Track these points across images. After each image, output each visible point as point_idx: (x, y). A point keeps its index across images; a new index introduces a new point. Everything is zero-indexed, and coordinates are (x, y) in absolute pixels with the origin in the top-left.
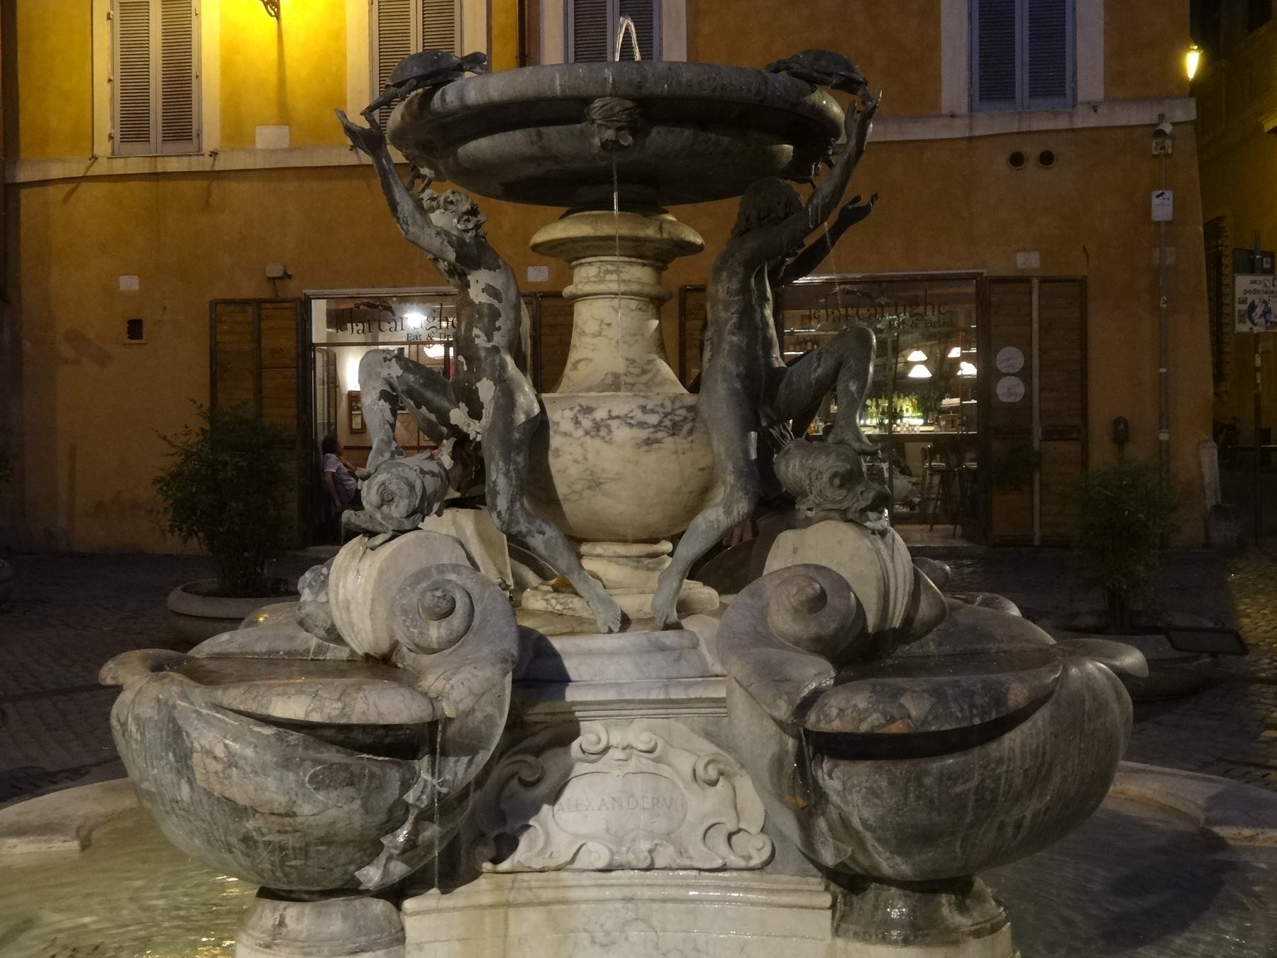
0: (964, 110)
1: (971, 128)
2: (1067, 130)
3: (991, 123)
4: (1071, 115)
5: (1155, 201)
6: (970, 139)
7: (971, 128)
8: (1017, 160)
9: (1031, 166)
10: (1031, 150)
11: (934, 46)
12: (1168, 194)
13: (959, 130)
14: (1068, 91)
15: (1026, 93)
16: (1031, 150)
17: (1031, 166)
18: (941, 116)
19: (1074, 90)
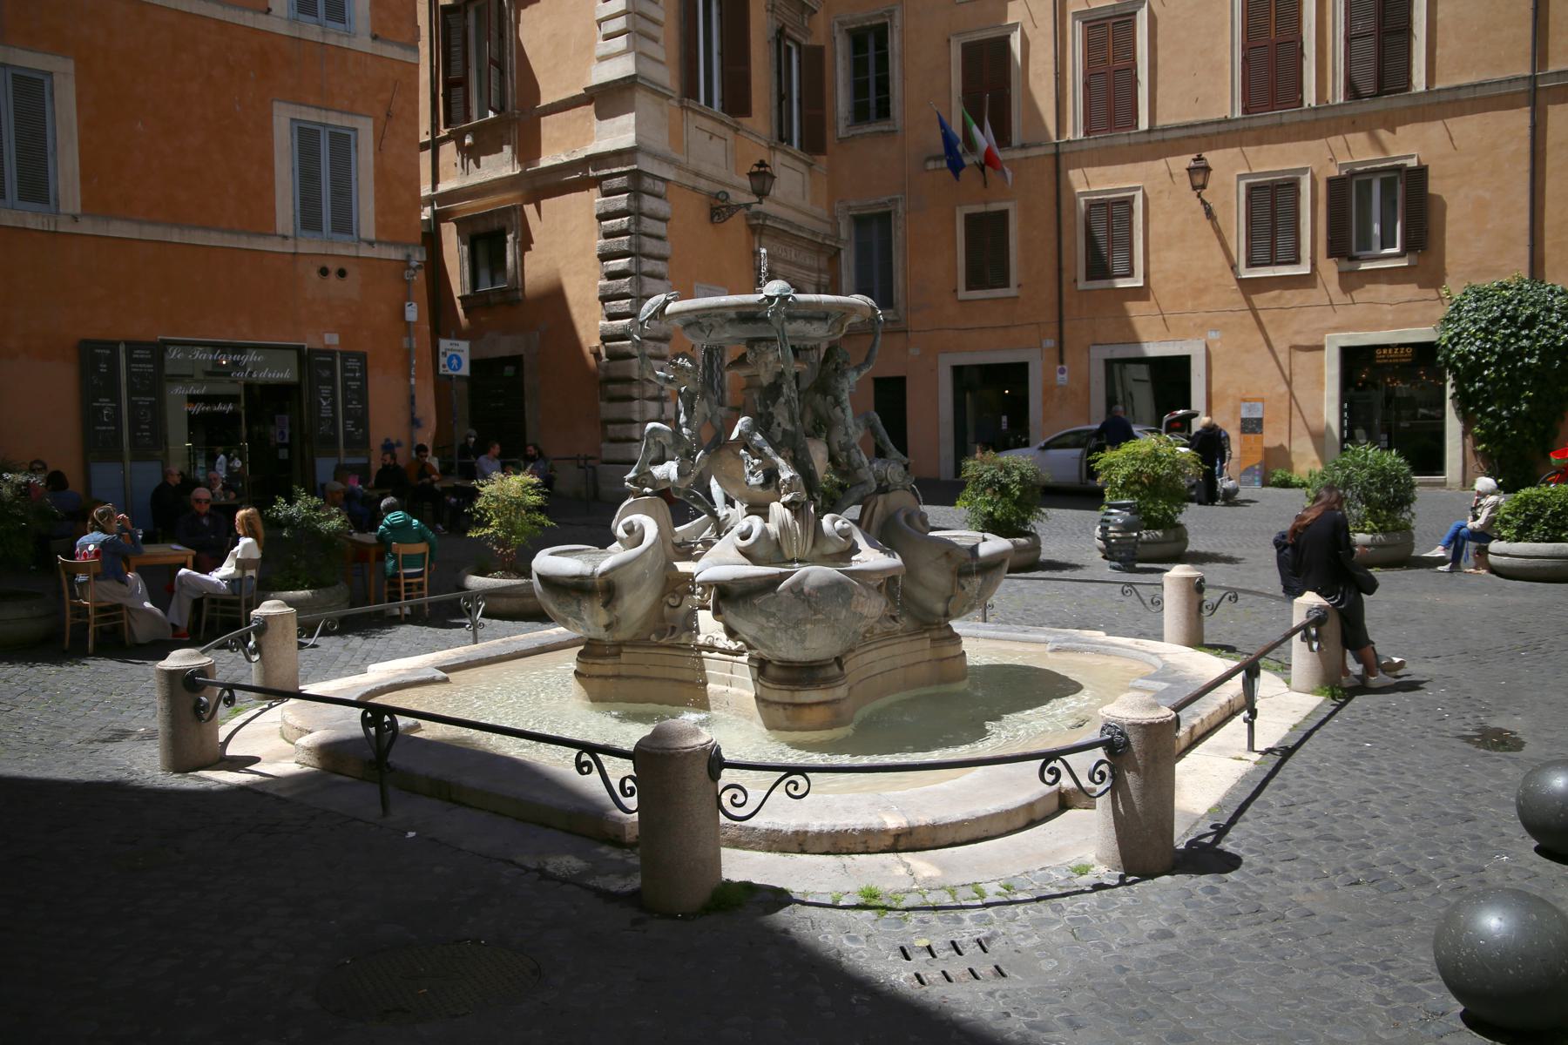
0: (290, 233)
1: (296, 246)
2: (354, 257)
3: (309, 245)
4: (357, 247)
5: (407, 309)
6: (294, 254)
7: (296, 246)
8: (324, 272)
9: (333, 277)
10: (333, 267)
11: (270, 187)
12: (414, 305)
13: (288, 248)
14: (354, 231)
15: (330, 229)
16: (333, 267)
17: (333, 277)
18: (276, 235)
19: (358, 230)
